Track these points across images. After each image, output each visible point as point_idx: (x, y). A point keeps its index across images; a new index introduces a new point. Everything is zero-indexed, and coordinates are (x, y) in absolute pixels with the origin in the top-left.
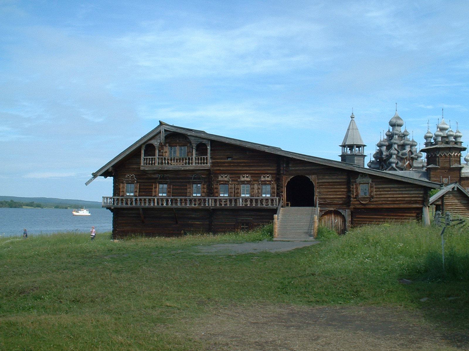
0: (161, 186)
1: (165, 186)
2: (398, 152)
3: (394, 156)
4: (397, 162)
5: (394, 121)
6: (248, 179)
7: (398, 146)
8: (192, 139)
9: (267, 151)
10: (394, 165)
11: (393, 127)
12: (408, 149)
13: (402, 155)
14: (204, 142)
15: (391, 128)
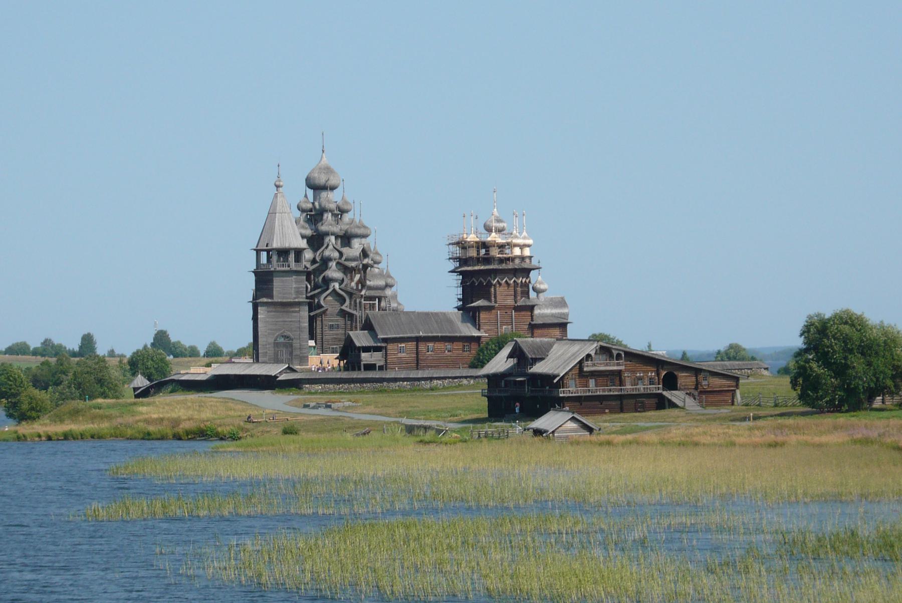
0: (591, 380)
1: (594, 380)
2: (341, 254)
3: (333, 264)
4: (343, 279)
5: (321, 179)
6: (642, 375)
7: (337, 237)
8: (613, 351)
9: (657, 357)
10: (337, 286)
11: (317, 192)
12: (357, 245)
13: (345, 260)
14: (621, 352)
15: (310, 193)
